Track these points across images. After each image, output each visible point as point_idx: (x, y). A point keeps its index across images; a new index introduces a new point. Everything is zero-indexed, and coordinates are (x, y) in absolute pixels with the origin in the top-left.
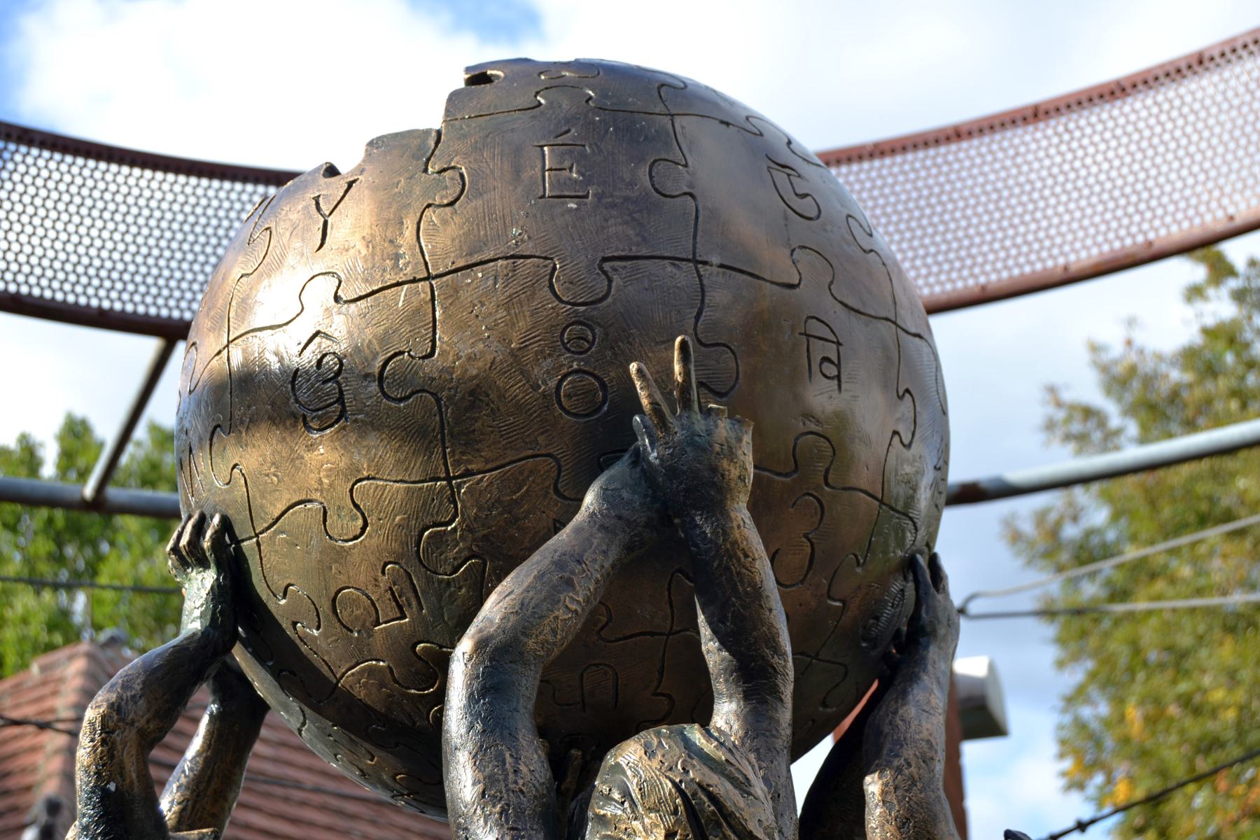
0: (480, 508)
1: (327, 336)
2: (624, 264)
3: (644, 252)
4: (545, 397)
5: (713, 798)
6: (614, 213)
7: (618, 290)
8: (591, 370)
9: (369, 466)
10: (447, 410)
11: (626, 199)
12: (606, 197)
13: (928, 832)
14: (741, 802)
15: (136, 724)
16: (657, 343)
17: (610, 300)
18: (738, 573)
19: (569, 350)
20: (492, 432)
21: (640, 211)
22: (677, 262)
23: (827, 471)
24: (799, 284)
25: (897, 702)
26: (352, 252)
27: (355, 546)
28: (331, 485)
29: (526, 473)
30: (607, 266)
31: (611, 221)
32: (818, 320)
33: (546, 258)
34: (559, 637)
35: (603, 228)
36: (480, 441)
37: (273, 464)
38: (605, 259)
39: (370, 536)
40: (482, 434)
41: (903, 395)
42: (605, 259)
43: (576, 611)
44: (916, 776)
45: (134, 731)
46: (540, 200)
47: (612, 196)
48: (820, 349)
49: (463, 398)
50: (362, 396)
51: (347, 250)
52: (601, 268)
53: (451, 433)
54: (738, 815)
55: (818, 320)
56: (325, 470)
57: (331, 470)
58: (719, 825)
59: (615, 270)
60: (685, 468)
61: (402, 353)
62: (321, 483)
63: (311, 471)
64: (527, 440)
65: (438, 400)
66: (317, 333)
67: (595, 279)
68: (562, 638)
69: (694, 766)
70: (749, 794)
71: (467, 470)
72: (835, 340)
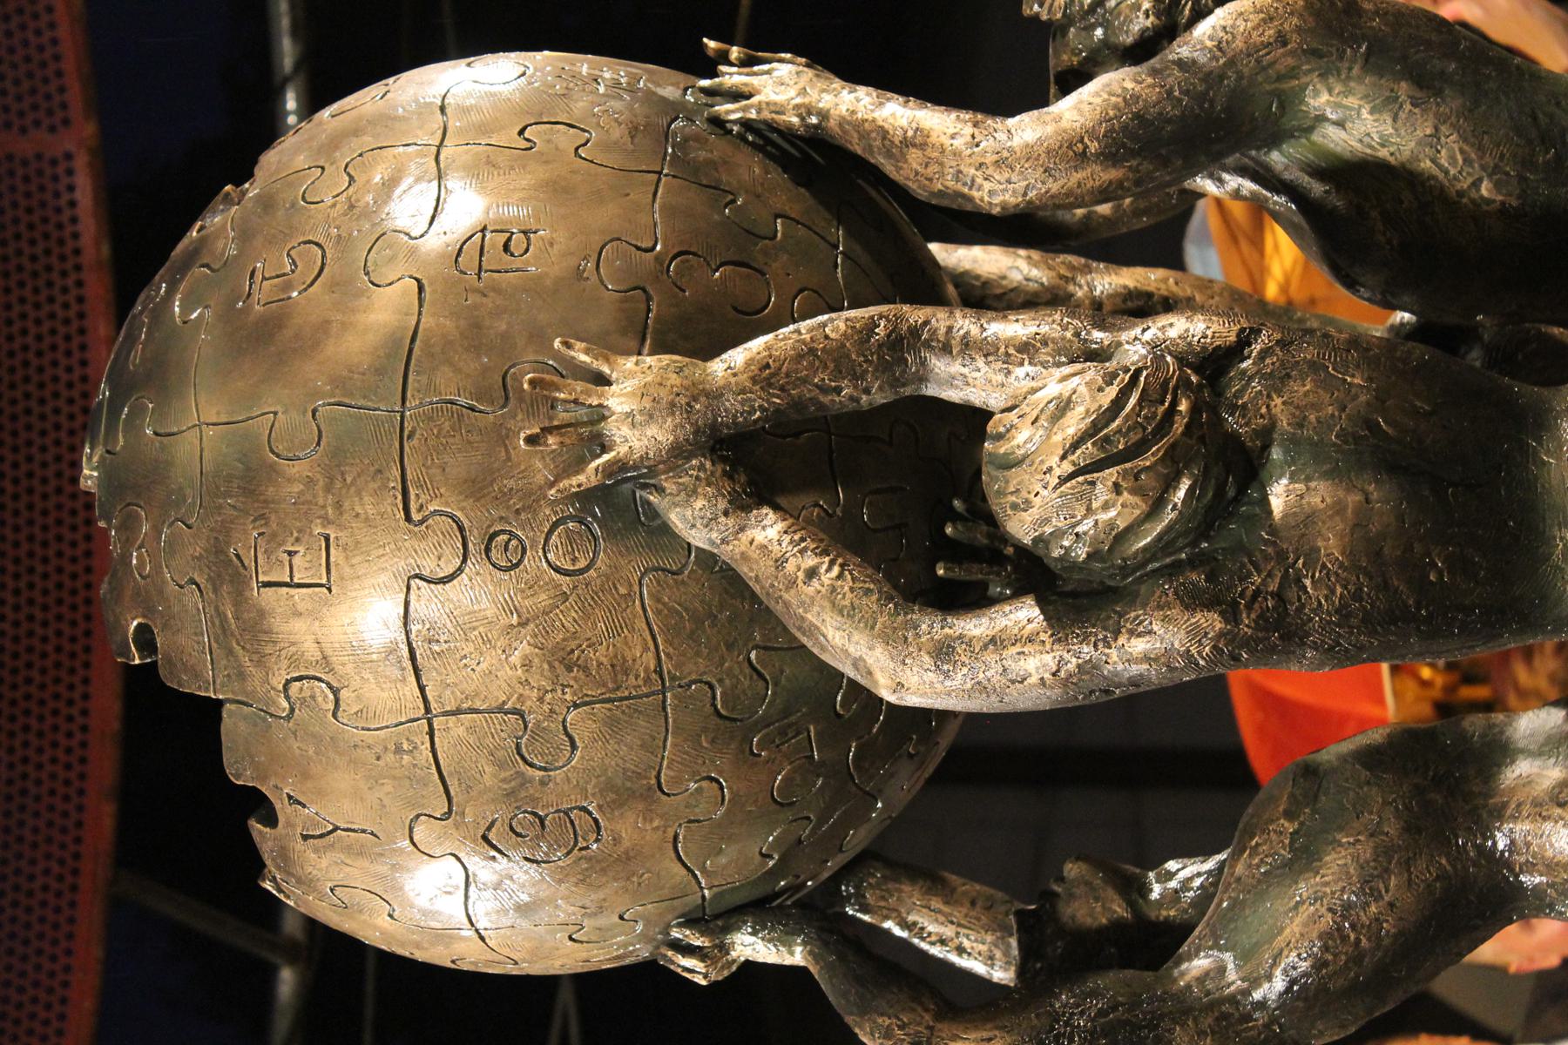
0: (698, 654)
1: (489, 829)
2: (413, 497)
3: (397, 474)
4: (575, 587)
5: (1075, 446)
6: (346, 505)
7: (447, 504)
8: (544, 536)
9: (646, 778)
10: (587, 695)
11: (328, 489)
12: (326, 514)
13: (1060, 147)
14: (1080, 410)
15: (931, 1024)
16: (509, 459)
17: (458, 514)
18: (787, 375)
19: (520, 562)
20: (614, 645)
21: (343, 474)
22: (406, 433)
23: (638, 248)
24: (417, 280)
25: (901, 168)
26: (386, 801)
27: (729, 788)
28: (661, 816)
29: (660, 606)
30: (416, 517)
31: (358, 509)
32: (459, 255)
33: (408, 588)
34: (872, 586)
35: (367, 519)
36: (624, 657)
37: (628, 879)
38: (408, 518)
39: (720, 773)
40: (616, 656)
41: (528, 140)
42: (408, 518)
43: (842, 566)
44: (996, 157)
45: (939, 1026)
46: (334, 591)
47: (324, 507)
48: (494, 257)
49: (575, 679)
50: (566, 788)
51: (384, 806)
52: (422, 522)
53: (618, 689)
54: (1094, 416)
55: (459, 255)
56: (644, 824)
57: (645, 819)
58: (1106, 439)
59: (421, 508)
60: (672, 438)
61: (518, 747)
62: (657, 828)
63: (643, 838)
64: (624, 606)
65: (576, 706)
66: (485, 838)
67: (434, 531)
68: (873, 581)
69: (1042, 462)
70: (1069, 400)
71: (655, 671)
72: (479, 234)
